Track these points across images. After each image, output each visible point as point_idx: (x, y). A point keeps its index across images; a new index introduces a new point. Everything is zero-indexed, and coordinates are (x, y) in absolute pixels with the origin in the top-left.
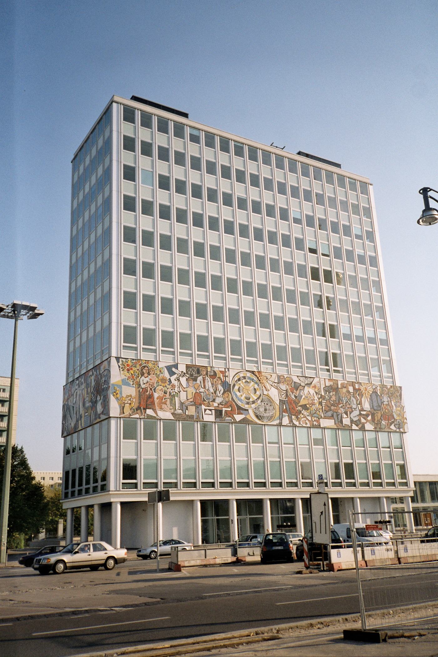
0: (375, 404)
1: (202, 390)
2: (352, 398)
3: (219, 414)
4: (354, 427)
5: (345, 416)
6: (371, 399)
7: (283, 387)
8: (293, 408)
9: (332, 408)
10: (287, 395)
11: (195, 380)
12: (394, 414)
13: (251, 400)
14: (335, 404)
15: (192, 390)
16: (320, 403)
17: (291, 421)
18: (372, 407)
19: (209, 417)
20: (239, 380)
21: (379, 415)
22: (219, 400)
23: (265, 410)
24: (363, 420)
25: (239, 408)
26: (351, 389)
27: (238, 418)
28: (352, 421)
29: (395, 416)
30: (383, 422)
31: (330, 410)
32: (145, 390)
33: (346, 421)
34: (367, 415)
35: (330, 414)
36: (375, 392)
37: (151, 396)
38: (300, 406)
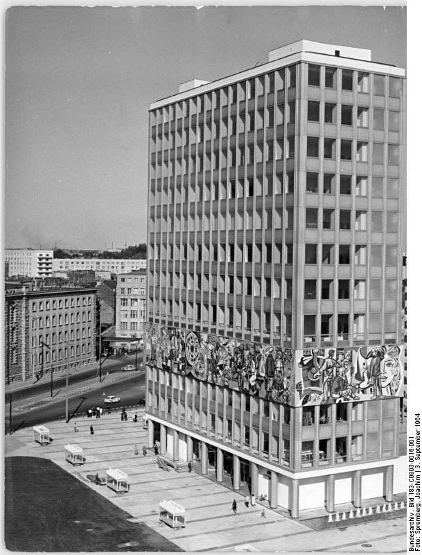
0: (270, 370)
1: (173, 348)
2: (253, 362)
5: (245, 379)
8: (215, 368)
9: (238, 370)
10: (212, 355)
11: (171, 339)
12: (284, 383)
13: (194, 357)
15: (169, 347)
16: (231, 366)
18: (266, 374)
20: (189, 340)
21: (271, 383)
22: (180, 356)
23: (200, 367)
24: (258, 387)
26: (252, 351)
29: (285, 387)
30: (273, 392)
31: (236, 372)
32: (153, 345)
33: (246, 386)
34: (262, 381)
35: (236, 375)
36: (270, 356)
37: (155, 351)
38: (219, 366)
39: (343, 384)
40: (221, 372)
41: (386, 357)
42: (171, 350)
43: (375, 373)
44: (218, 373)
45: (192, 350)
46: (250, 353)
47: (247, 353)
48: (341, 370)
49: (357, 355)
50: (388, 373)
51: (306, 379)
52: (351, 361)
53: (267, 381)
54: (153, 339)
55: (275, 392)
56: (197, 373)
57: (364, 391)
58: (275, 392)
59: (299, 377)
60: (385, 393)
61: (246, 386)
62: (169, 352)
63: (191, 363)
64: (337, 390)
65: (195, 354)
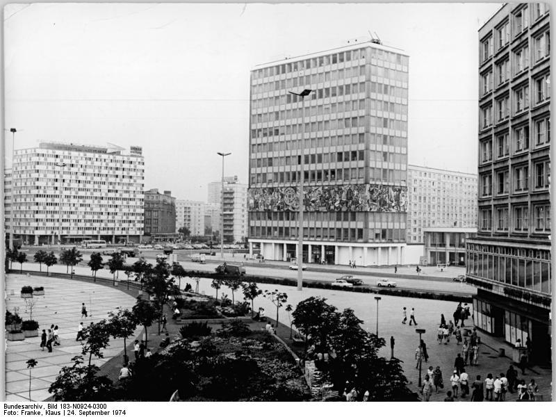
0: (349, 196)
3: (279, 208)
4: (336, 210)
6: (347, 194)
7: (305, 193)
14: (328, 199)
15: (270, 199)
16: (320, 199)
17: (306, 209)
18: (347, 198)
19: (276, 210)
21: (350, 202)
25: (287, 205)
26: (336, 189)
27: (286, 209)
28: (335, 207)
29: (360, 202)
33: (332, 207)
36: (350, 189)
39: (385, 203)
40: (313, 204)
41: (402, 192)
42: (272, 201)
43: (397, 199)
44: (311, 205)
45: (290, 196)
46: (335, 191)
47: (332, 191)
48: (384, 196)
49: (390, 189)
50: (403, 200)
51: (371, 198)
52: (388, 192)
53: (347, 203)
54: (256, 196)
55: (353, 207)
56: (294, 208)
57: (393, 207)
58: (353, 207)
59: (369, 198)
60: (402, 210)
61: (332, 207)
62: (270, 201)
63: (288, 204)
64: (383, 206)
65: (291, 199)
